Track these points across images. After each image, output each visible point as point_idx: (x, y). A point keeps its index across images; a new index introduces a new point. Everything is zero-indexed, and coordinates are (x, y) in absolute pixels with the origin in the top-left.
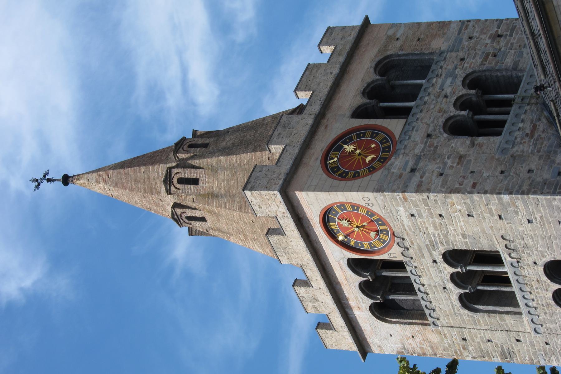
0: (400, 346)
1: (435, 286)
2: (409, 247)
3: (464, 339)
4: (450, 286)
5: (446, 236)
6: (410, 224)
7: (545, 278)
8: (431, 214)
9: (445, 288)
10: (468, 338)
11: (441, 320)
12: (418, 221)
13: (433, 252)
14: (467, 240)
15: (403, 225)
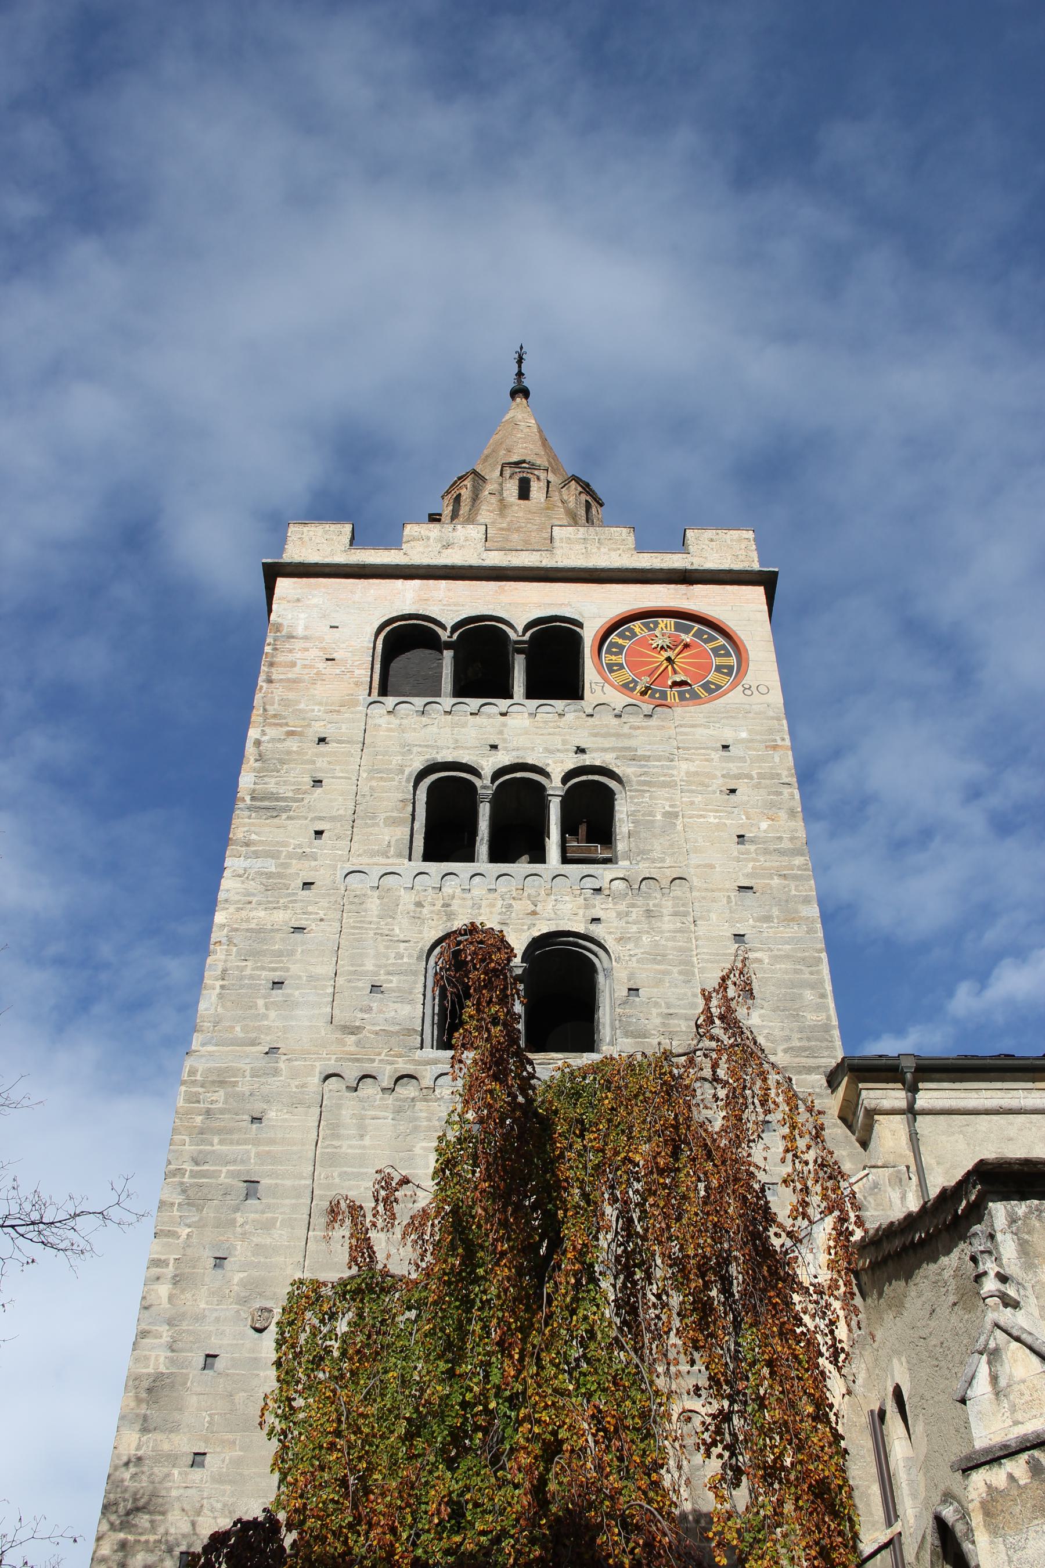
0: (300, 631)
1: (501, 732)
2: (623, 719)
3: (322, 740)
4: (503, 759)
5: (670, 785)
6: (697, 737)
7: (544, 928)
8: (738, 777)
9: (494, 747)
10: (322, 747)
11: (387, 717)
12: (713, 753)
13: (614, 755)
14: (659, 817)
15: (693, 726)
